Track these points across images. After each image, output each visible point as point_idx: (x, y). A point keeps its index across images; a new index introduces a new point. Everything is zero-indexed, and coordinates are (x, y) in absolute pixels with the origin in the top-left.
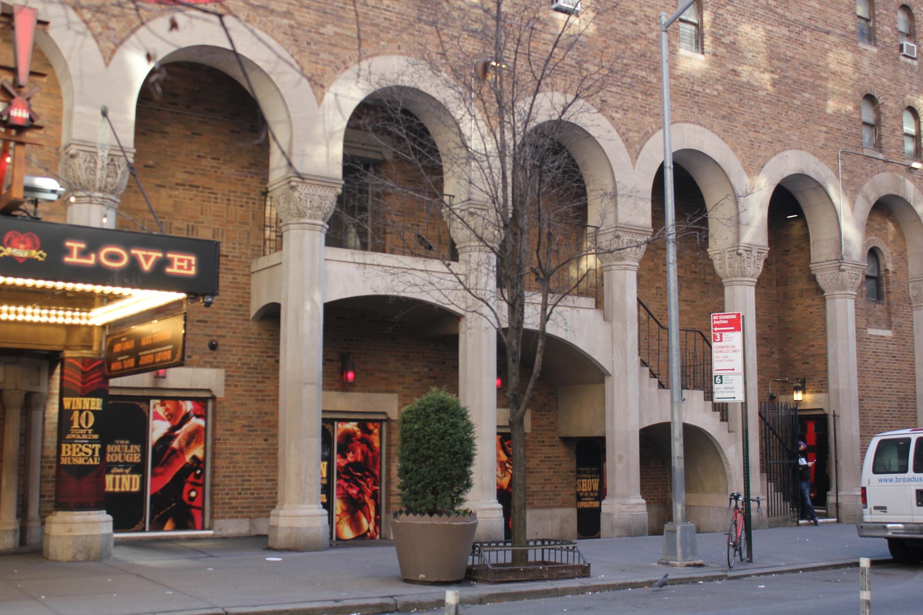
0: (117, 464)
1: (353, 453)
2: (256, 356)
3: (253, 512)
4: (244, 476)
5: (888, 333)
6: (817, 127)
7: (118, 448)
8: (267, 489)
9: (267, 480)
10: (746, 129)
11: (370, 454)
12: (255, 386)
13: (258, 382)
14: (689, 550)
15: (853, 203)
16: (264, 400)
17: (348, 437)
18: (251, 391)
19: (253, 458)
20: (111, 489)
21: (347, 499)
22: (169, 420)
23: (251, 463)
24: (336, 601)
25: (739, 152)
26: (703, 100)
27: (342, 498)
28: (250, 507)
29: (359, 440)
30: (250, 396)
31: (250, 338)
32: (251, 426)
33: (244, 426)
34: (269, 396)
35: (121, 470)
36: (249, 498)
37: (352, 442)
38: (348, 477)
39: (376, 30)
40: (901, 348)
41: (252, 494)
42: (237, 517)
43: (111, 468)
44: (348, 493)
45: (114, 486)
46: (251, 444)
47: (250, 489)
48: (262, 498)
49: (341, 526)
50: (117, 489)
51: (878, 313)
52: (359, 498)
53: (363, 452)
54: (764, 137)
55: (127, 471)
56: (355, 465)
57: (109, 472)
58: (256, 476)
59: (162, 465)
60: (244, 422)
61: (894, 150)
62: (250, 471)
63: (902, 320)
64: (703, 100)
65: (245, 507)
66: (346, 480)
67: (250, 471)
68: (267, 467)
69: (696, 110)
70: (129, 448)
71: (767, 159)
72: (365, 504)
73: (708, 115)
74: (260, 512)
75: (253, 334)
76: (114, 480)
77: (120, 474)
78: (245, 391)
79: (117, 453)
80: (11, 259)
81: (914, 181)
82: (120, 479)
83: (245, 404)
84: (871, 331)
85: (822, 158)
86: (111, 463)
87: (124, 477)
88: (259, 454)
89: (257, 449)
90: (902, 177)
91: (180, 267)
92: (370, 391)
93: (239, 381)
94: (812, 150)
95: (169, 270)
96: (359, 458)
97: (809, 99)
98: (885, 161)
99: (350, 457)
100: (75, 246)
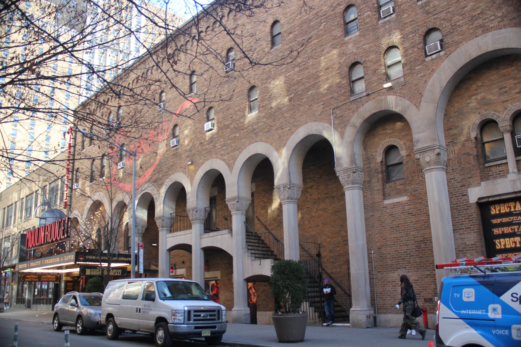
5: (404, 199)
6: (317, 105)
10: (277, 131)
15: (342, 135)
25: (274, 144)
26: (257, 130)
40: (417, 206)
51: (398, 187)
54: (286, 129)
61: (376, 84)
63: (418, 186)
64: (257, 130)
69: (254, 136)
71: (288, 139)
73: (260, 136)
81: (395, 94)
84: (387, 202)
85: (321, 120)
90: (383, 97)
94: (314, 119)
97: (311, 94)
98: (368, 95)
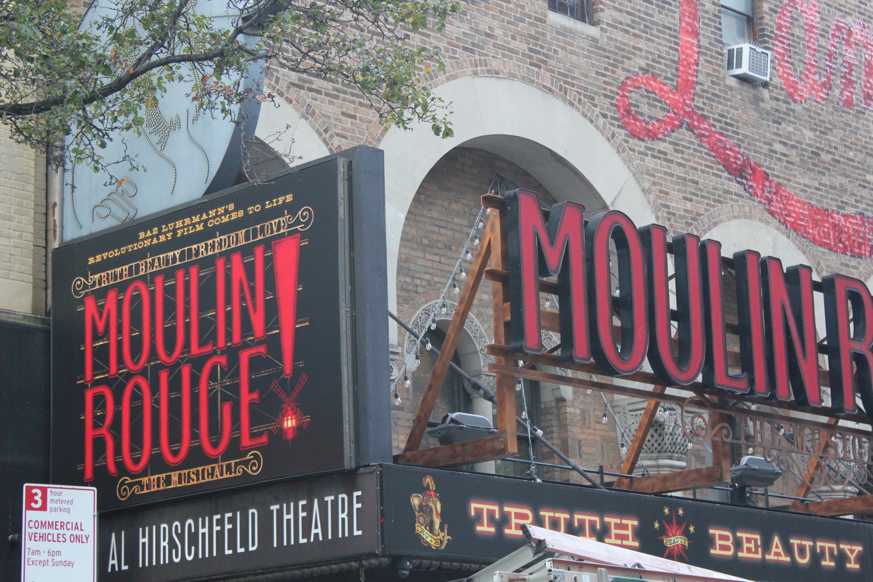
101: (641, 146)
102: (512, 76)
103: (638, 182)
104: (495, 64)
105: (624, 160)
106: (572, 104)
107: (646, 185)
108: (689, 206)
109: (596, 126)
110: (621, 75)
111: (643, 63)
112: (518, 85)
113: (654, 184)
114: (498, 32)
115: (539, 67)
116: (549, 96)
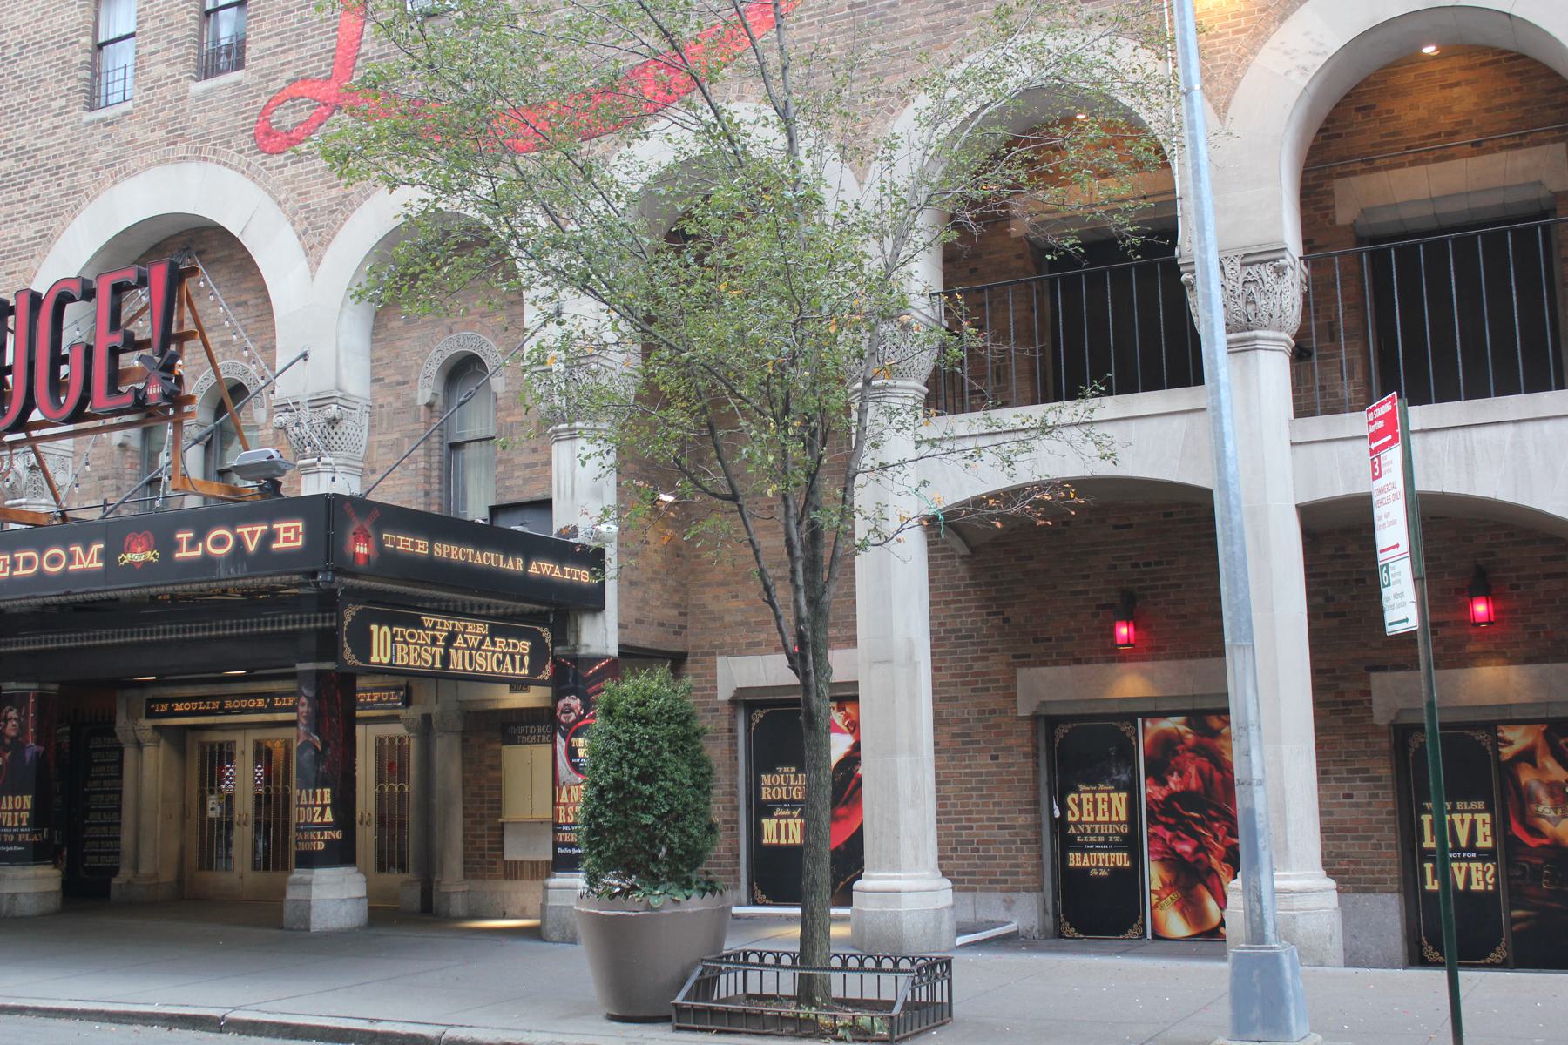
0: (782, 801)
1: (1181, 775)
2: (970, 616)
3: (979, 882)
4: (960, 820)
7: (780, 779)
8: (1001, 843)
9: (1000, 827)
11: (1217, 775)
12: (971, 667)
13: (975, 659)
14: (1256, 1013)
16: (988, 690)
17: (1166, 746)
18: (965, 675)
19: (973, 789)
20: (775, 841)
21: (1172, 861)
22: (852, 732)
23: (970, 797)
24: (372, 1021)
27: (1162, 860)
28: (973, 873)
29: (1190, 750)
30: (963, 684)
31: (958, 587)
32: (969, 735)
33: (955, 736)
34: (997, 681)
35: (788, 812)
36: (970, 858)
37: (1176, 753)
38: (1171, 821)
39: (956, 15)
41: (977, 850)
42: (974, 890)
43: (774, 809)
44: (1173, 850)
45: (779, 837)
46: (969, 766)
47: (972, 842)
48: (994, 858)
49: (1161, 914)
50: (783, 841)
52: (1198, 861)
53: (1200, 772)
55: (796, 813)
56: (1185, 798)
57: (770, 815)
58: (981, 820)
59: (846, 803)
60: (956, 729)
62: (971, 812)
65: (965, 873)
66: (1167, 826)
67: (971, 812)
68: (999, 804)
70: (796, 778)
72: (1211, 871)
74: (991, 882)
75: (962, 578)
76: (778, 826)
77: (786, 817)
78: (953, 676)
79: (780, 786)
80: (131, 564)
82: (787, 825)
83: (956, 699)
86: (773, 801)
87: (791, 822)
88: (983, 782)
89: (981, 774)
91: (287, 540)
92: (1191, 657)
93: (944, 661)
95: (274, 546)
96: (1193, 785)
99: (1174, 783)
100: (184, 536)
101: (280, 159)
102: (149, 166)
103: (274, 198)
104: (132, 165)
105: (260, 184)
106: (206, 159)
107: (282, 197)
108: (334, 192)
109: (231, 167)
110: (263, 101)
111: (290, 75)
112: (156, 171)
113: (293, 190)
114: (141, 137)
115: (174, 143)
116: (185, 166)
